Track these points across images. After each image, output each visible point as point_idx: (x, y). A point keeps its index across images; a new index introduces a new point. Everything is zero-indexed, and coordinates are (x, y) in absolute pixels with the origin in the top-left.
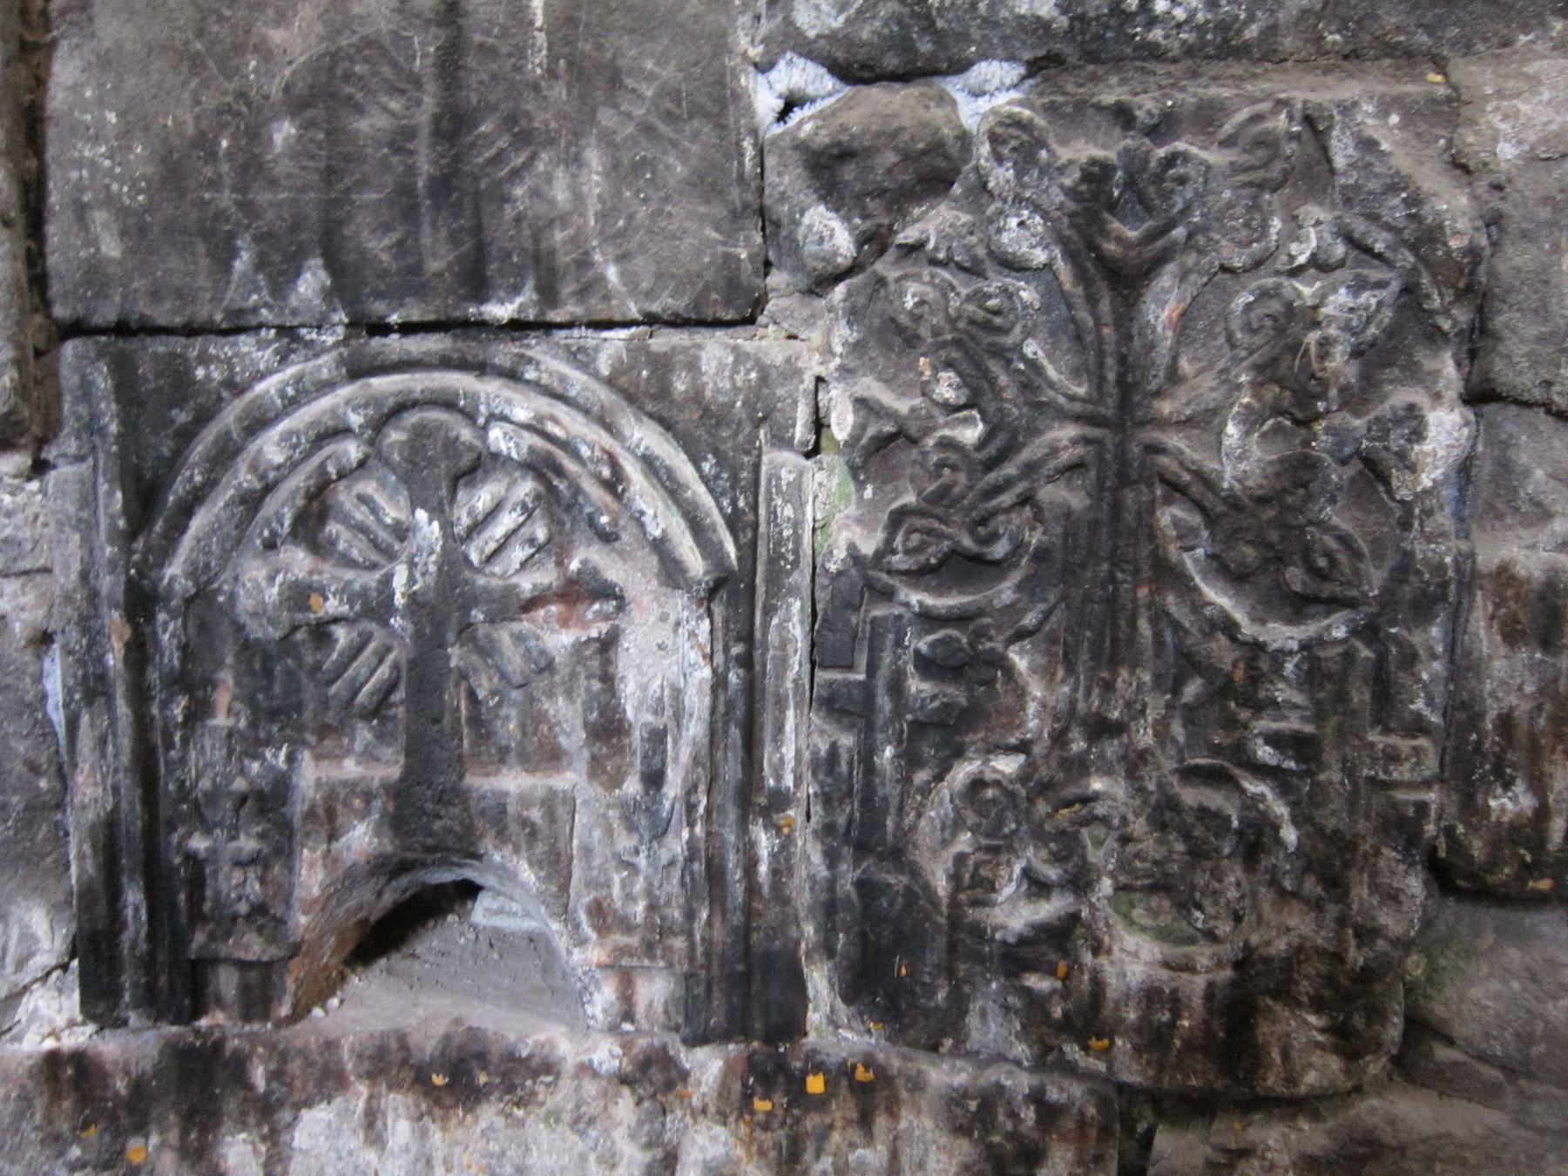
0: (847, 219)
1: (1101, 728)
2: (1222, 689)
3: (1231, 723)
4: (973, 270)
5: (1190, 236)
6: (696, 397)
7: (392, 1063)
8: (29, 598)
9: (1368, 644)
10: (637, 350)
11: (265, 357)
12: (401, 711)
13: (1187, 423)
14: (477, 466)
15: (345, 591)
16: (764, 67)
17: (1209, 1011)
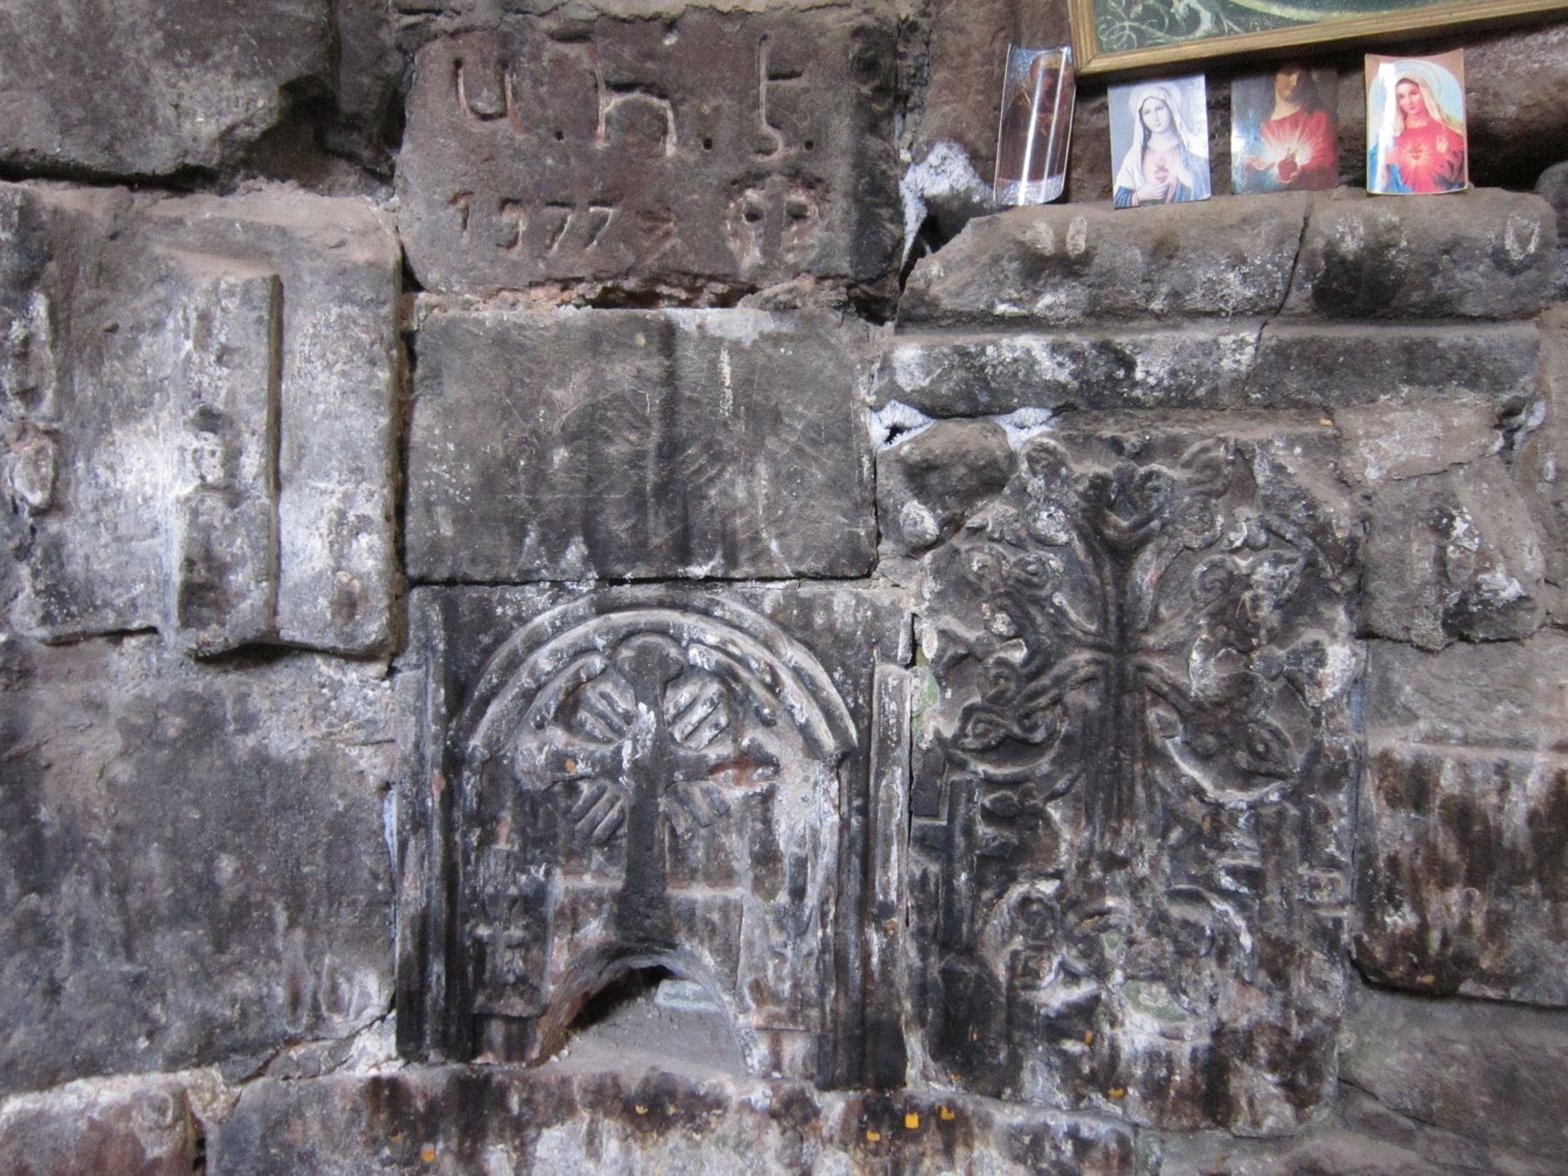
0: (933, 510)
1: (1112, 862)
2: (1194, 835)
3: (1202, 859)
4: (1019, 545)
5: (1163, 526)
6: (830, 628)
7: (607, 1097)
8: (378, 760)
9: (1296, 804)
10: (790, 596)
11: (541, 601)
12: (624, 842)
13: (1165, 651)
14: (682, 673)
15: (590, 758)
16: (877, 408)
17: (1194, 1069)
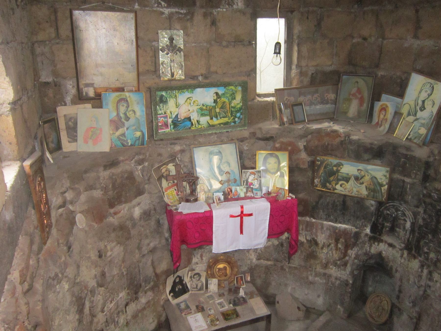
14: (400, 210)
